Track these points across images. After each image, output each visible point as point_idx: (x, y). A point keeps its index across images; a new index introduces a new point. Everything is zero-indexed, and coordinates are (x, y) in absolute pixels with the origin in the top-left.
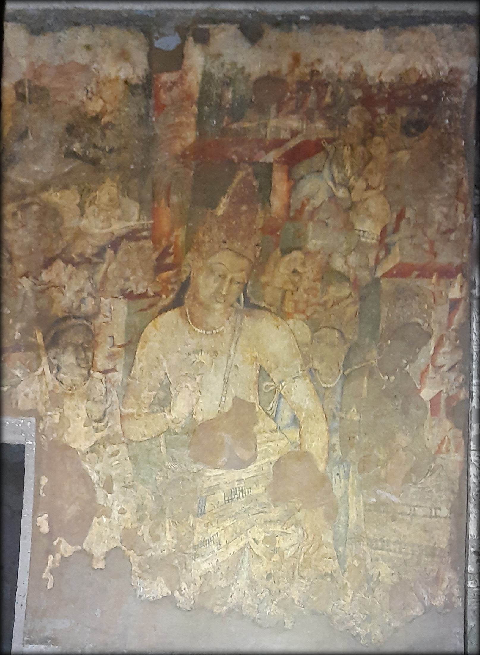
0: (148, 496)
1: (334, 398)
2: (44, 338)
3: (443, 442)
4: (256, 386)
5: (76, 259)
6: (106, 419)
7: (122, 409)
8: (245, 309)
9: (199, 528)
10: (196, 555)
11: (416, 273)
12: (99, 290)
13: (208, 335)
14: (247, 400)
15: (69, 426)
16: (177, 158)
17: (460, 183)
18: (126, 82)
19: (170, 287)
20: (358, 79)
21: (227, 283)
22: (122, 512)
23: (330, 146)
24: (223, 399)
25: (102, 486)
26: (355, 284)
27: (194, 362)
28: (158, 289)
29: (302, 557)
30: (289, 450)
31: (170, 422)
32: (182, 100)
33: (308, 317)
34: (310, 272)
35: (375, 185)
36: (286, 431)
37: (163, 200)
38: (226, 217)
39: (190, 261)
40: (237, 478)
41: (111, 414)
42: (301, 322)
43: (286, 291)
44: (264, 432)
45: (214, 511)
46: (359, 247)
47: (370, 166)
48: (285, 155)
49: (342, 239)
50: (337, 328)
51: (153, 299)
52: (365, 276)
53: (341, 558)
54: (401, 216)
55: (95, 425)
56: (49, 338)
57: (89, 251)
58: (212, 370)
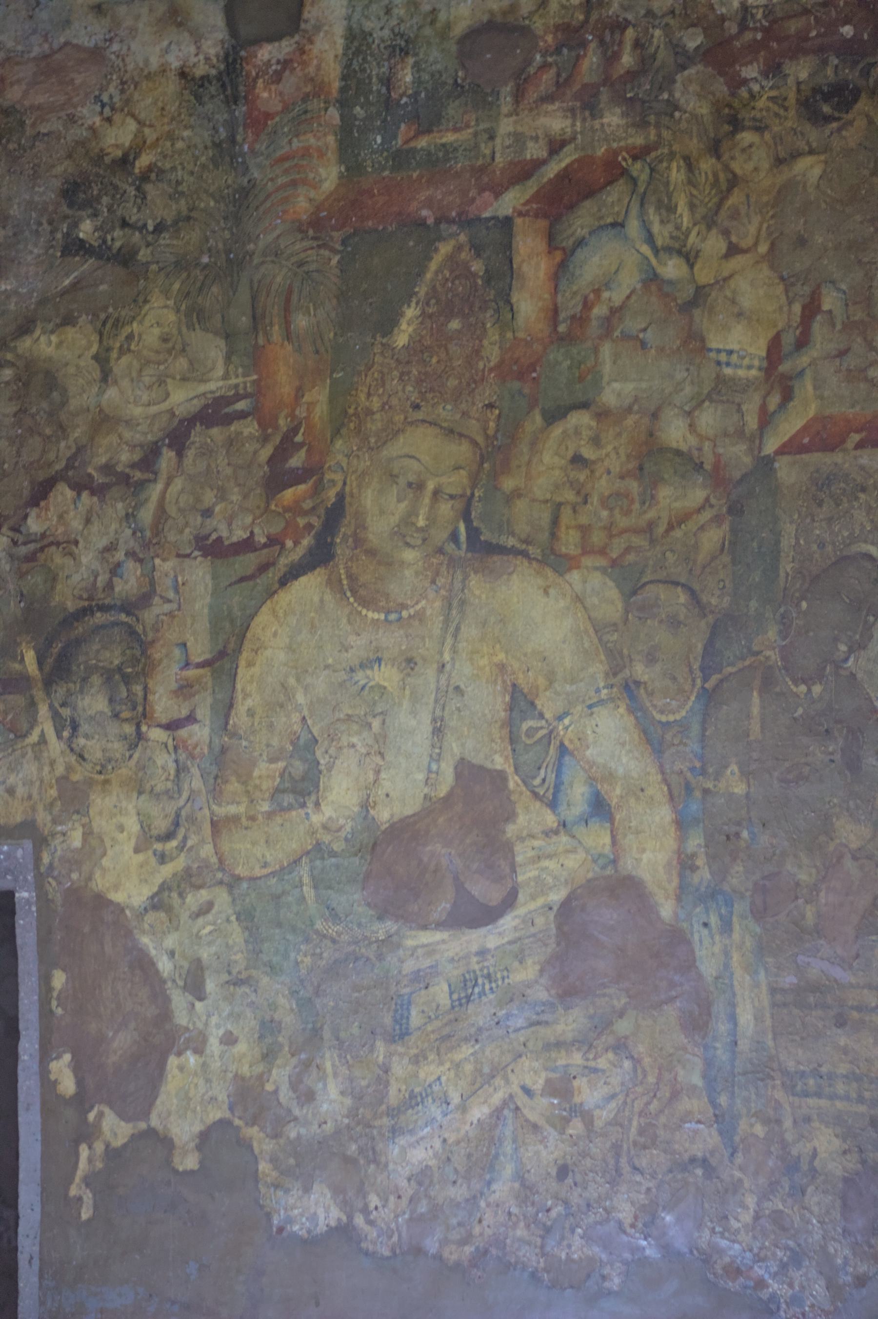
0: (282, 1001)
1: (685, 745)
2: (40, 663)
4: (505, 732)
5: (99, 479)
6: (181, 832)
7: (215, 807)
8: (469, 555)
9: (400, 1068)
10: (395, 1131)
11: (856, 437)
12: (150, 544)
13: (390, 622)
14: (489, 765)
15: (104, 854)
16: (300, 229)
18: (182, 74)
19: (301, 522)
21: (427, 501)
22: (229, 1040)
23: (638, 165)
24: (434, 767)
25: (181, 983)
26: (717, 477)
27: (363, 688)
28: (275, 528)
29: (635, 1123)
30: (590, 875)
31: (321, 831)
32: (305, 98)
33: (614, 563)
35: (744, 244)
36: (580, 831)
37: (276, 327)
38: (418, 349)
39: (340, 457)
40: (474, 948)
41: (192, 819)
42: (598, 574)
43: (560, 505)
44: (532, 836)
45: (429, 1028)
46: (722, 390)
47: (735, 199)
48: (535, 197)
49: (680, 375)
50: (683, 580)
51: (265, 551)
52: (738, 455)
53: (723, 1121)
54: (811, 309)
55: (158, 846)
56: (50, 660)
57: (125, 457)
58: (406, 704)
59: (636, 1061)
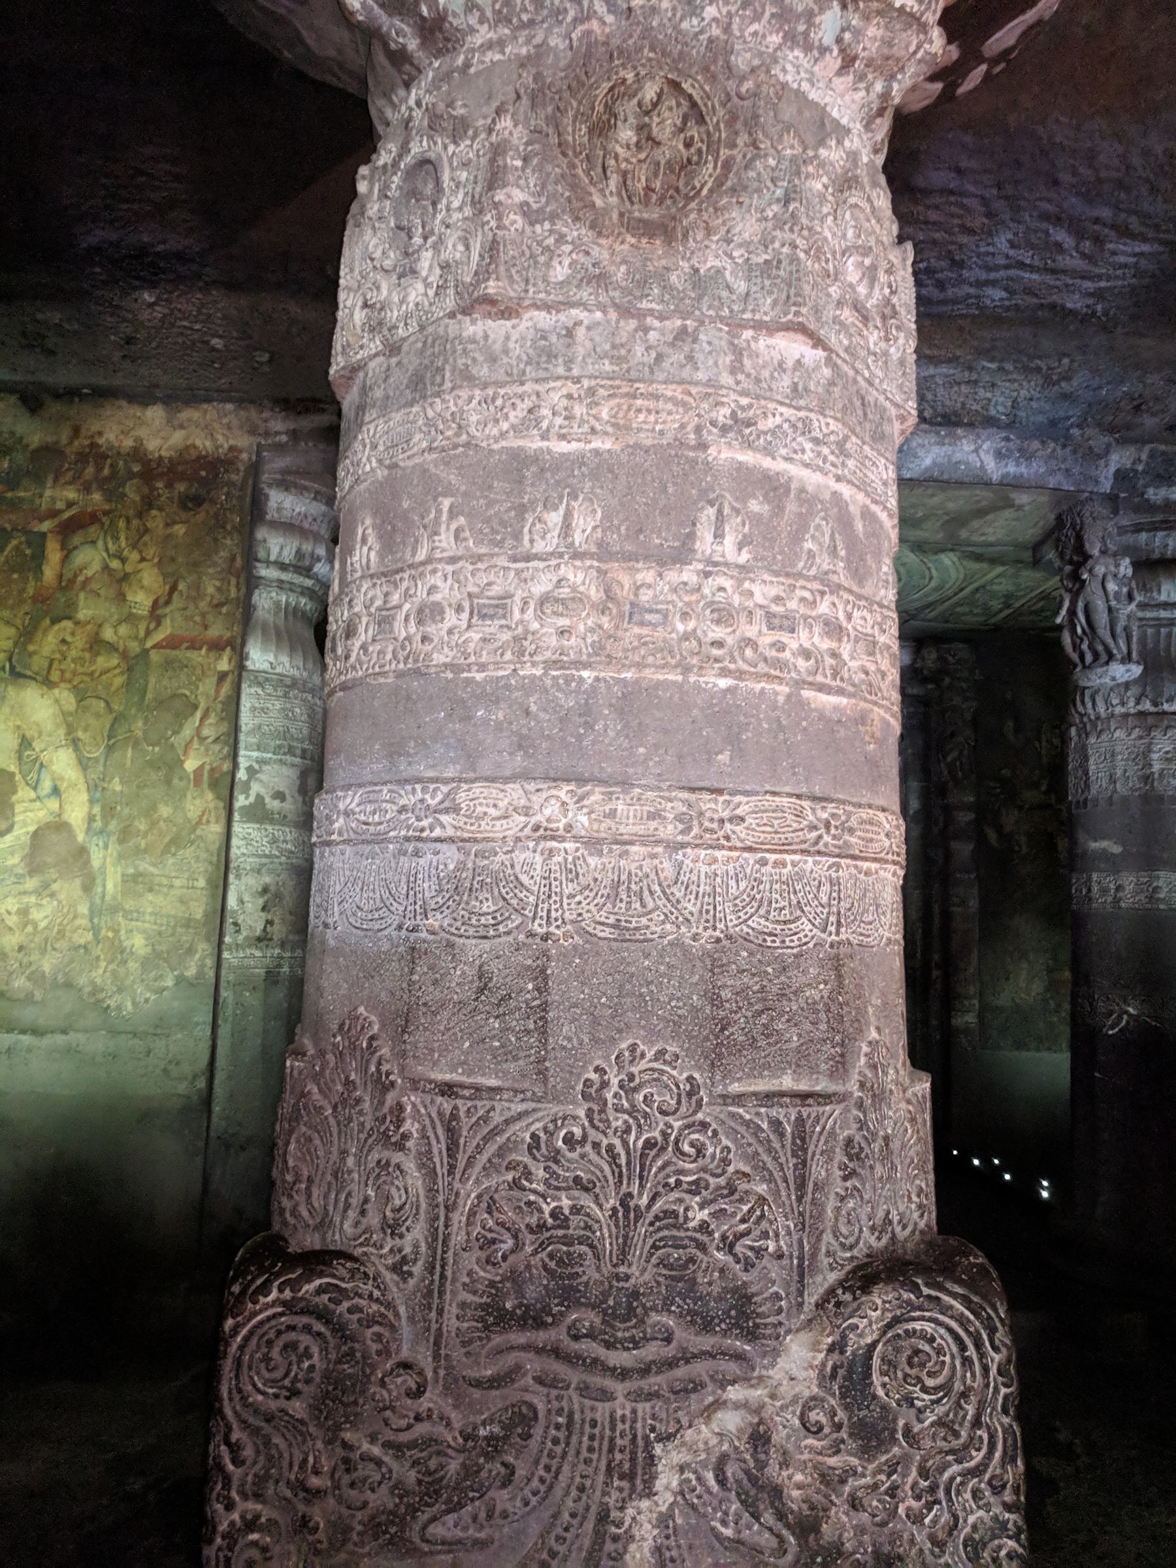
3: (203, 813)
11: (185, 645)
17: (233, 559)
20: (137, 453)
26: (124, 655)
34: (79, 642)
36: (46, 801)
46: (130, 618)
47: (146, 538)
48: (60, 525)
52: (134, 647)
53: (96, 930)
59: (60, 902)
